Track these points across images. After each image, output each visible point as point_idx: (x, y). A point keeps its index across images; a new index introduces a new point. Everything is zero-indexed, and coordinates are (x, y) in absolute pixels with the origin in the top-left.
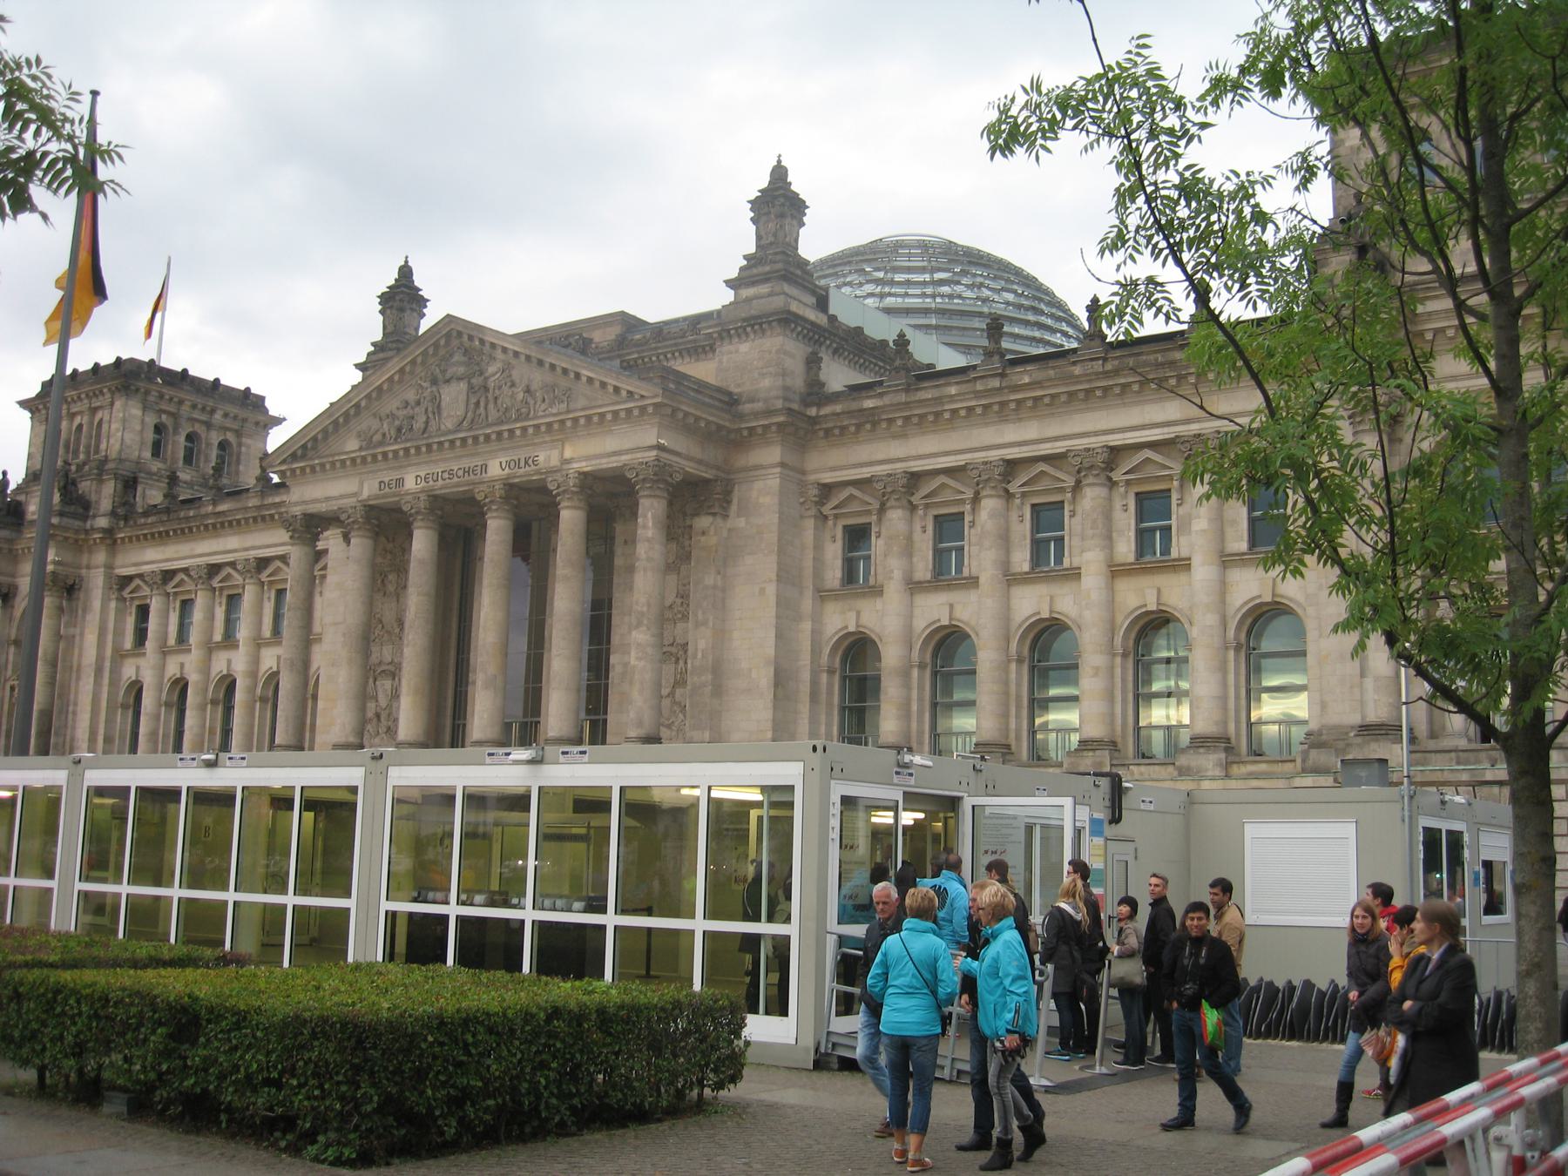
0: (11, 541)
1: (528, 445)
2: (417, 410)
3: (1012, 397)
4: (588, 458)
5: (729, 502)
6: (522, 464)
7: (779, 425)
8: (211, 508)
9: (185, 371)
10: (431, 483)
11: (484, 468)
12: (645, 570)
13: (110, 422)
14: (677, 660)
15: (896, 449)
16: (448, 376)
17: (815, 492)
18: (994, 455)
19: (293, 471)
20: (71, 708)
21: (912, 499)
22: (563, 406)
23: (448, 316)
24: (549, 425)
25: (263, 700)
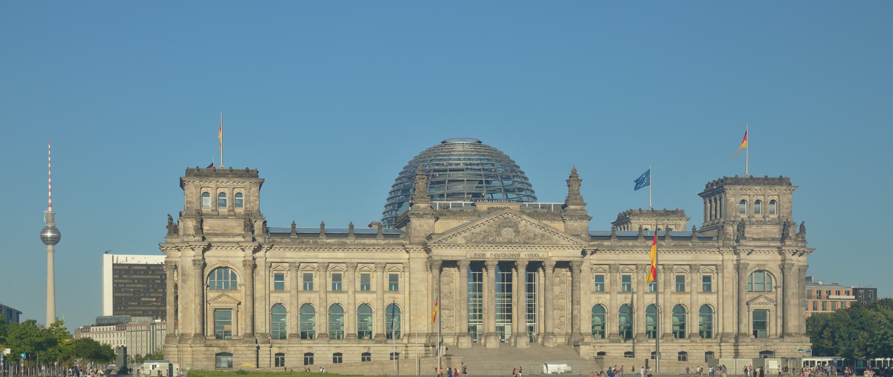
2: (490, 234)
6: (533, 255)
8: (325, 240)
11: (519, 255)
13: (249, 196)
16: (505, 224)
18: (644, 263)
22: (550, 241)
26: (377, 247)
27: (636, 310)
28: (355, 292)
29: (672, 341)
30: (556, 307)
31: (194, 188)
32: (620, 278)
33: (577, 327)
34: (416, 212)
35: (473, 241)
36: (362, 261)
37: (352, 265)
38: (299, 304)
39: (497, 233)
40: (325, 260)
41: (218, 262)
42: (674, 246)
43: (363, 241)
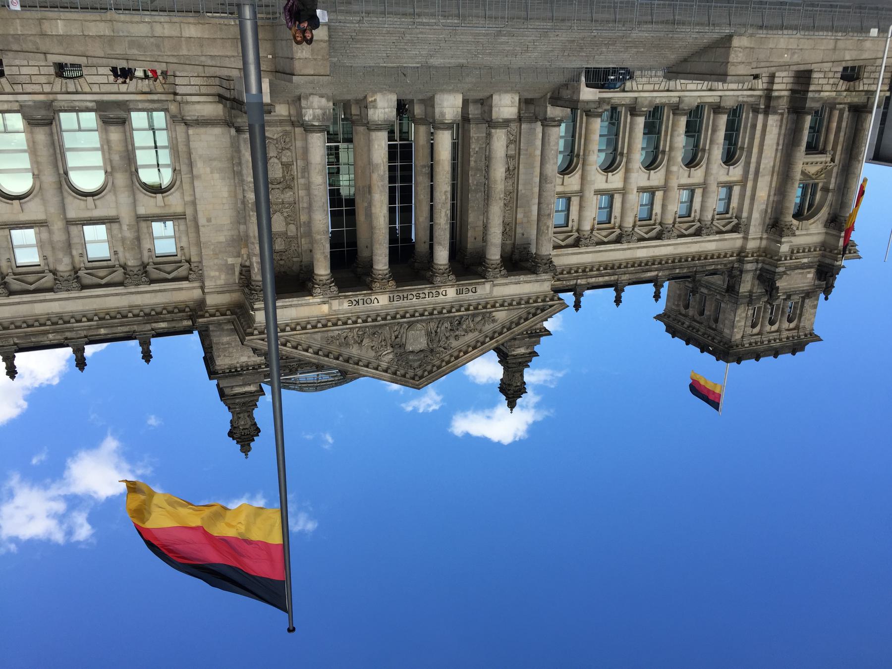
0: (823, 256)
2: (448, 334)
4: (308, 304)
5: (241, 274)
6: (361, 302)
7: (203, 316)
8: (660, 274)
9: (702, 352)
10: (434, 291)
12: (254, 237)
15: (138, 300)
17: (190, 277)
20: (780, 147)
21: (123, 270)
22: (330, 334)
23: (419, 389)
24: (335, 324)
27: (64, 183)
28: (624, 192)
30: (278, 186)
31: (807, 327)
34: (534, 339)
35: (480, 318)
36: (612, 246)
37: (629, 238)
38: (704, 166)
39: (437, 339)
41: (811, 227)
43: (607, 278)
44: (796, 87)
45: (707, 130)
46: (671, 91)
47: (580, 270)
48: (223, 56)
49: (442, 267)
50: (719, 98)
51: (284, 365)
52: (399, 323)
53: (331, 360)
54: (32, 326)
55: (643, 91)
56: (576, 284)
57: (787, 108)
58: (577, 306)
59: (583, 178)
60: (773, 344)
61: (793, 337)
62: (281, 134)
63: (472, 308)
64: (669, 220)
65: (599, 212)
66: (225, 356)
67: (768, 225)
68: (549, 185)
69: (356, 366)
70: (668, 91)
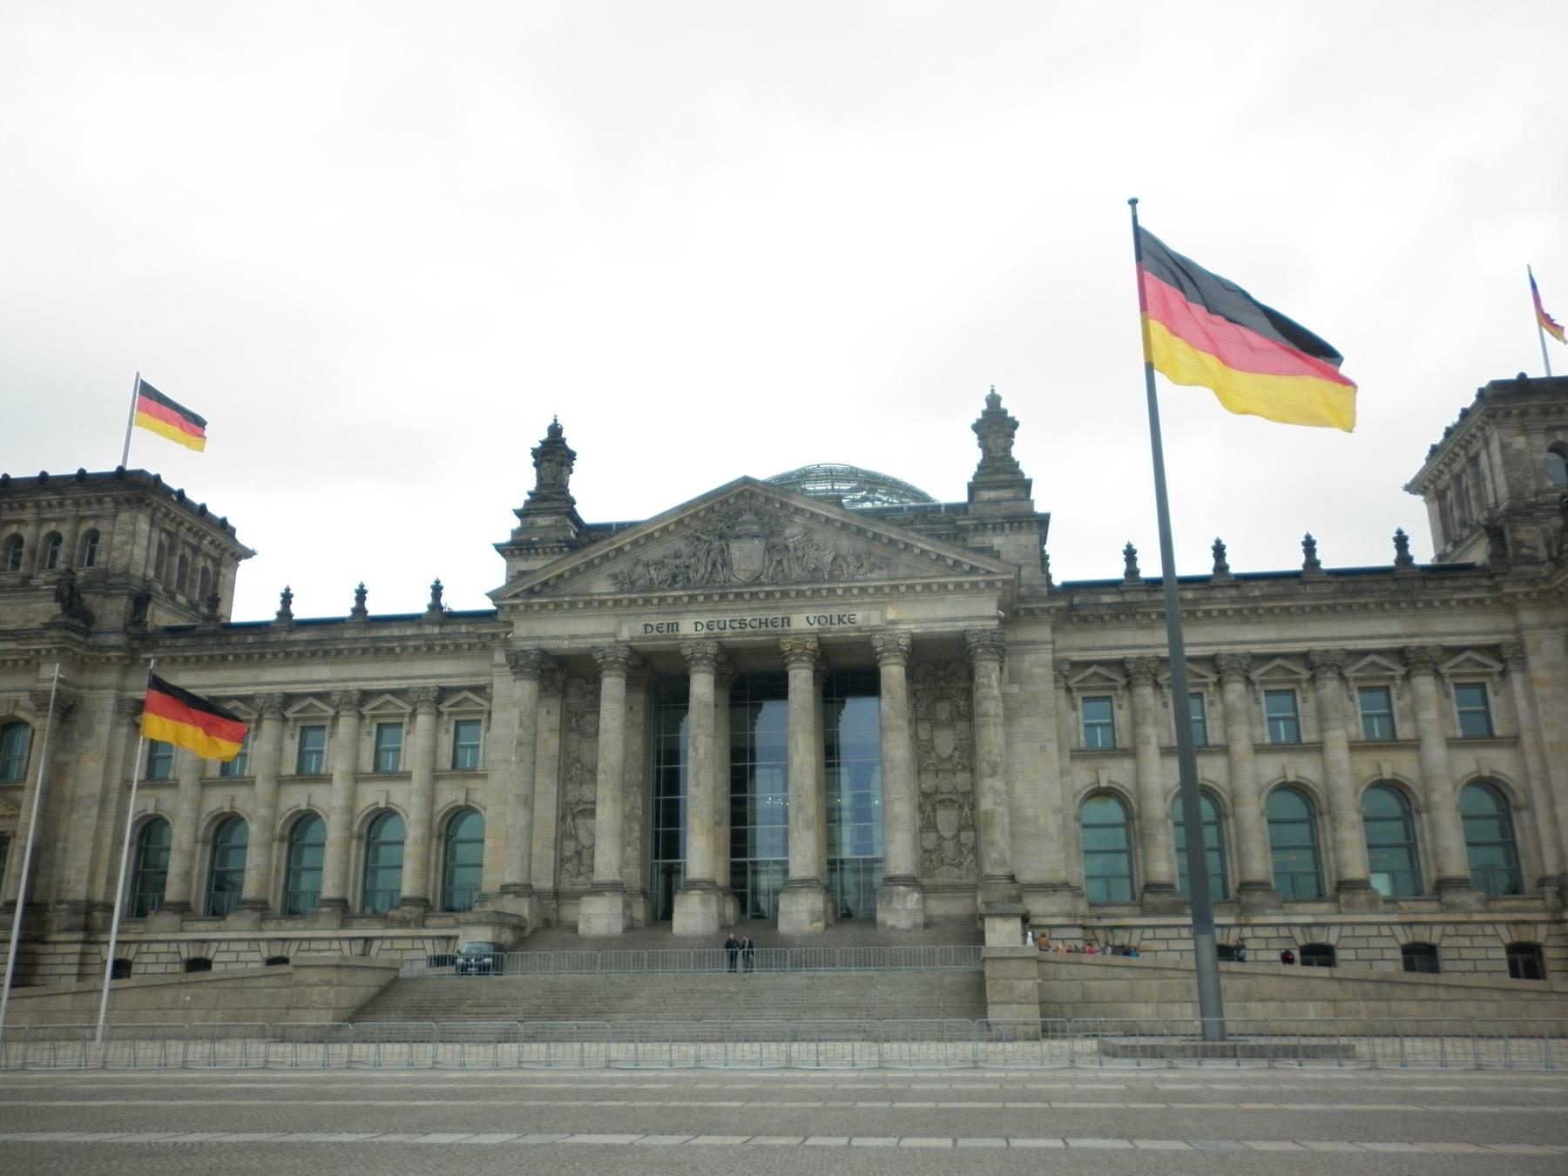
1: (841, 605)
2: (693, 560)
3: (1264, 605)
4: (917, 621)
6: (835, 620)
7: (1059, 609)
10: (716, 630)
12: (995, 725)
13: (111, 533)
14: (961, 807)
15: (1142, 637)
17: (1068, 667)
18: (1239, 649)
19: (528, 606)
20: (60, 845)
22: (884, 573)
24: (879, 589)
25: (360, 837)
26: (410, 643)
27: (1228, 803)
29: (1373, 903)
30: (944, 797)
32: (1165, 705)
33: (994, 855)
38: (204, 815)
39: (712, 554)
40: (276, 689)
42: (1336, 592)
43: (385, 633)
44: (40, 948)
45: (200, 875)
46: (278, 939)
47: (438, 649)
48: (1104, 979)
49: (702, 668)
50: (185, 928)
51: (936, 526)
52: (777, 584)
53: (886, 534)
54: (1282, 608)
55: (330, 939)
56: (442, 625)
57: (48, 911)
58: (437, 590)
59: (432, 800)
60: (54, 498)
61: (11, 508)
62: (937, 872)
63: (655, 601)
64: (269, 727)
65: (400, 742)
66: (1027, 547)
67: (77, 711)
68: (521, 791)
69: (847, 520)
70: (284, 940)
